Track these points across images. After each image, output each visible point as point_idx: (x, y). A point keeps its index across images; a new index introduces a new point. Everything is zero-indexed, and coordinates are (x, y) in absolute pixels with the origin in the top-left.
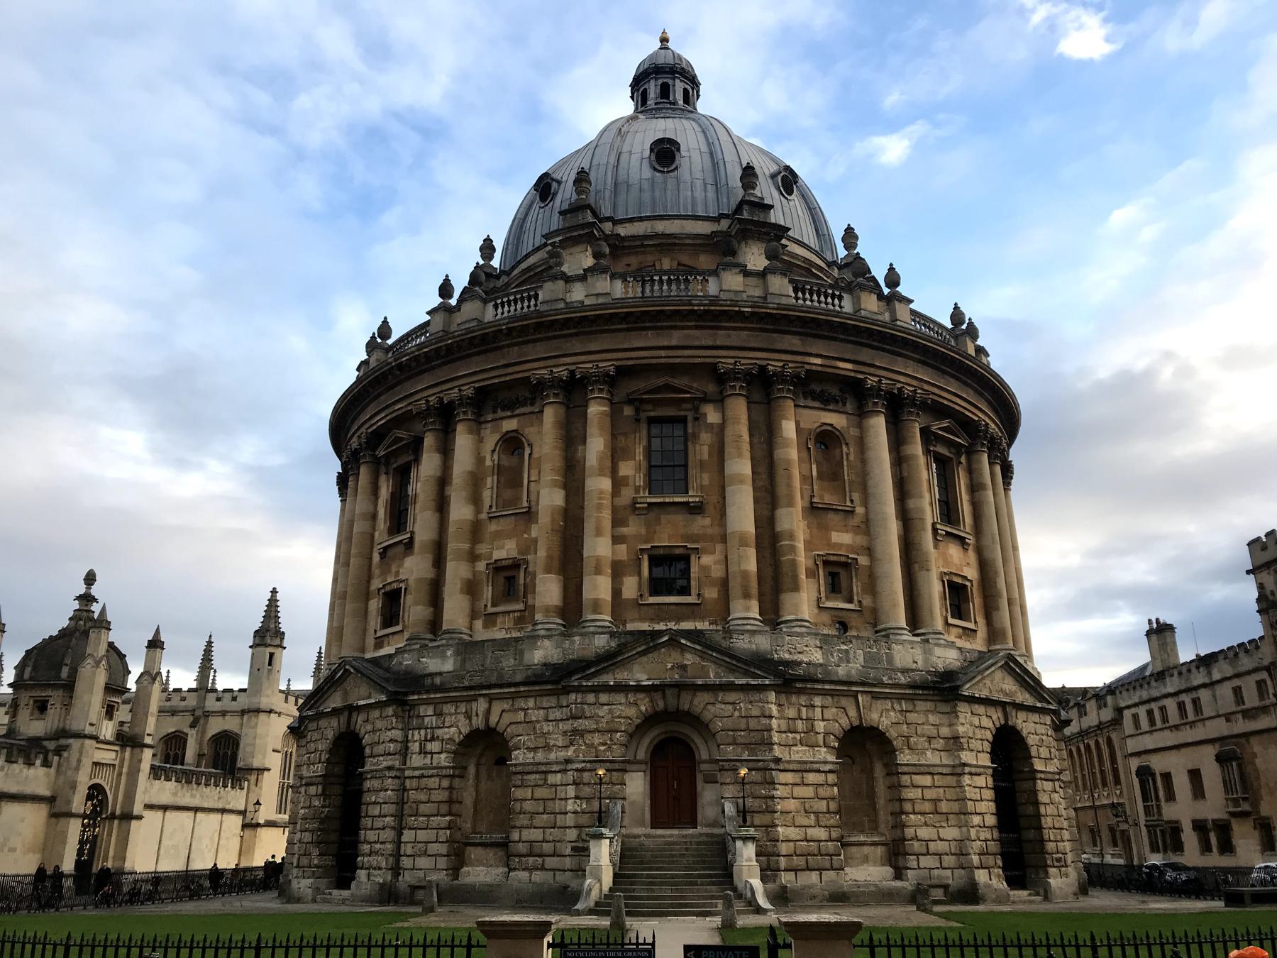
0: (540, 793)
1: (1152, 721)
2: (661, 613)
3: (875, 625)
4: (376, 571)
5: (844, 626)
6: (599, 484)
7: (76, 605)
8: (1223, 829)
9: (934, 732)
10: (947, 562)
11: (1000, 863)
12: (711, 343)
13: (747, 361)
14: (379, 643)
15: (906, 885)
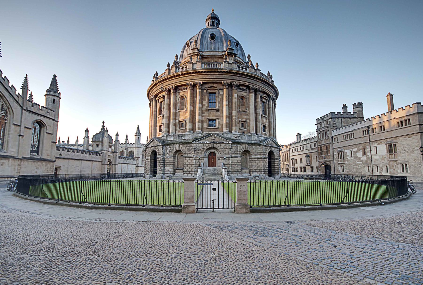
0: (189, 161)
1: (295, 151)
4: (157, 122)
5: (244, 133)
7: (102, 127)
8: (305, 168)
10: (263, 121)
13: (229, 82)
14: (159, 135)
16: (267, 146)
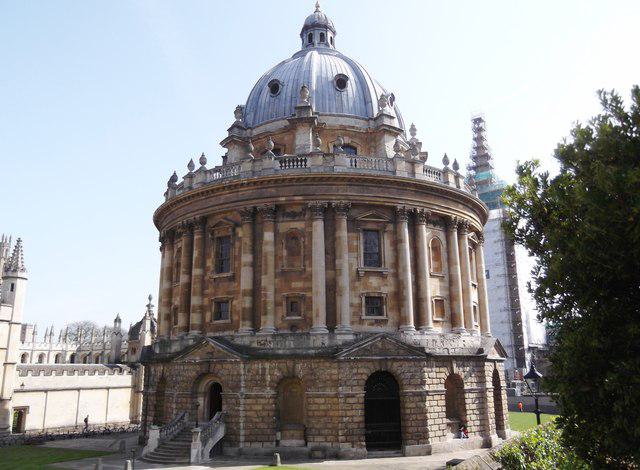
2: (218, 329)
3: (311, 325)
6: (196, 272)
9: (328, 377)
10: (366, 286)
11: (363, 438)
12: (236, 199)
15: (306, 449)
16: (355, 360)
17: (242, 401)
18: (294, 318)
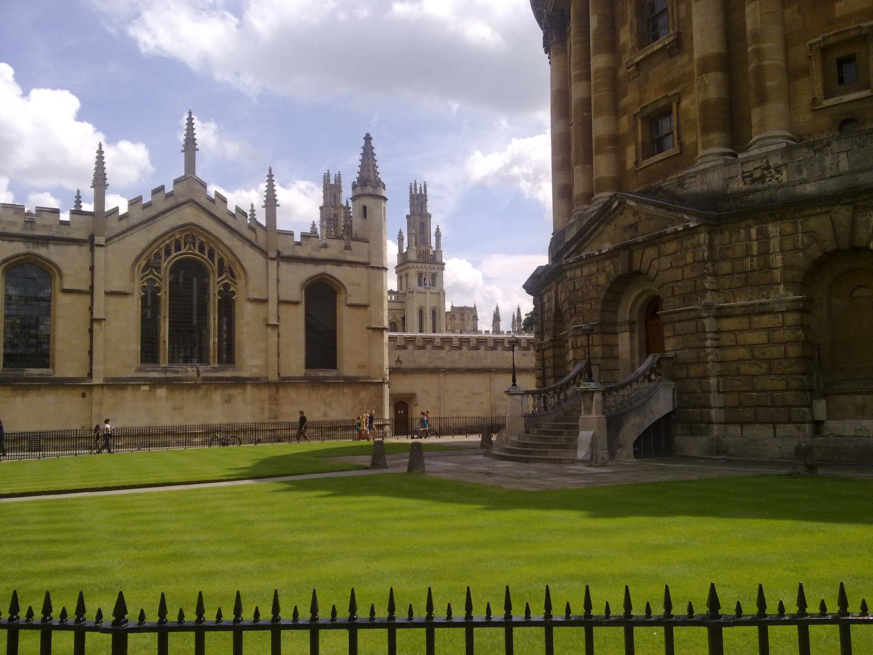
17: (709, 324)
18: (847, 98)
